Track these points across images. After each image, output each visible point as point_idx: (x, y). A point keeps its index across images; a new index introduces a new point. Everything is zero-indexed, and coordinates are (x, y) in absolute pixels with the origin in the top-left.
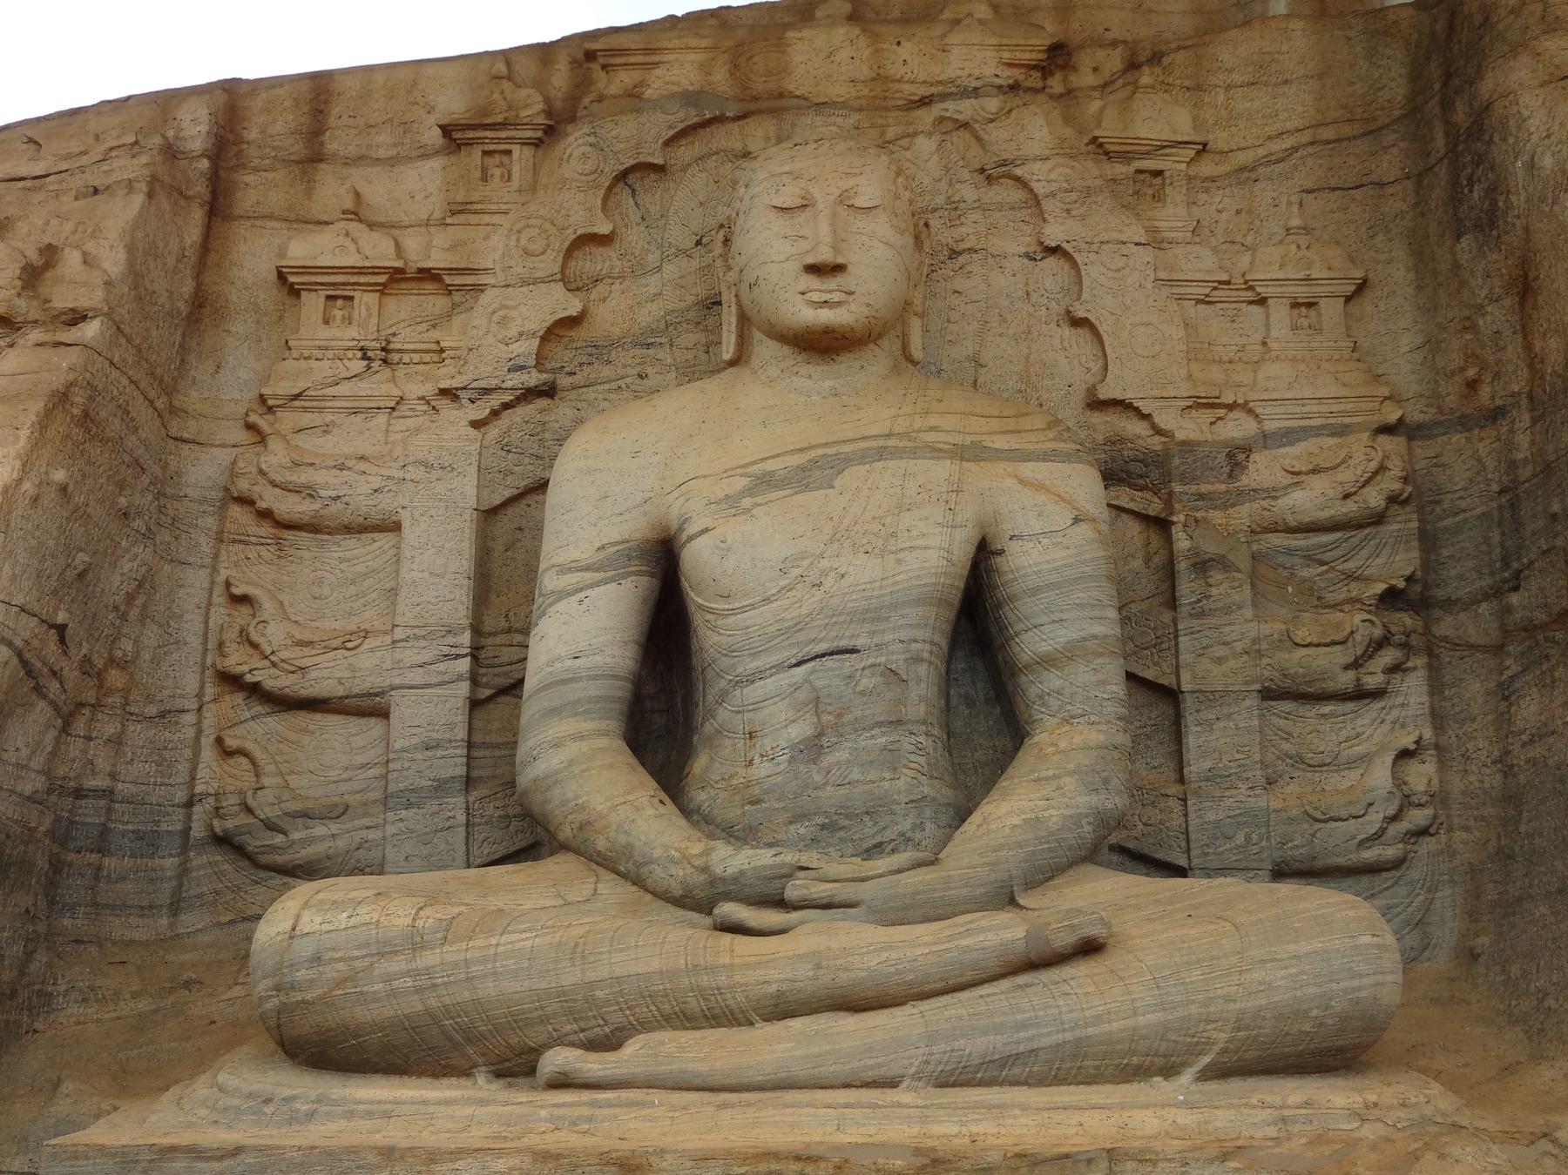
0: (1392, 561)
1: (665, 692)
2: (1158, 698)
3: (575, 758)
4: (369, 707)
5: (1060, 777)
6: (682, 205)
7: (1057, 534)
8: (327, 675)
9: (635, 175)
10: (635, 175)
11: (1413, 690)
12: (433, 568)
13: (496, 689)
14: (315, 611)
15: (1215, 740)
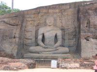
0: (74, 34)
1: (43, 40)
2: (63, 39)
3: (41, 43)
4: (31, 39)
5: (59, 43)
6: (45, 17)
7: (59, 33)
8: (29, 38)
9: (42, 16)
10: (42, 16)
11: (75, 39)
12: (34, 33)
13: (36, 38)
14: (28, 35)
15: (66, 41)
